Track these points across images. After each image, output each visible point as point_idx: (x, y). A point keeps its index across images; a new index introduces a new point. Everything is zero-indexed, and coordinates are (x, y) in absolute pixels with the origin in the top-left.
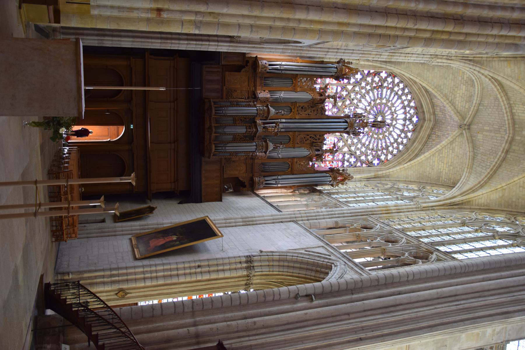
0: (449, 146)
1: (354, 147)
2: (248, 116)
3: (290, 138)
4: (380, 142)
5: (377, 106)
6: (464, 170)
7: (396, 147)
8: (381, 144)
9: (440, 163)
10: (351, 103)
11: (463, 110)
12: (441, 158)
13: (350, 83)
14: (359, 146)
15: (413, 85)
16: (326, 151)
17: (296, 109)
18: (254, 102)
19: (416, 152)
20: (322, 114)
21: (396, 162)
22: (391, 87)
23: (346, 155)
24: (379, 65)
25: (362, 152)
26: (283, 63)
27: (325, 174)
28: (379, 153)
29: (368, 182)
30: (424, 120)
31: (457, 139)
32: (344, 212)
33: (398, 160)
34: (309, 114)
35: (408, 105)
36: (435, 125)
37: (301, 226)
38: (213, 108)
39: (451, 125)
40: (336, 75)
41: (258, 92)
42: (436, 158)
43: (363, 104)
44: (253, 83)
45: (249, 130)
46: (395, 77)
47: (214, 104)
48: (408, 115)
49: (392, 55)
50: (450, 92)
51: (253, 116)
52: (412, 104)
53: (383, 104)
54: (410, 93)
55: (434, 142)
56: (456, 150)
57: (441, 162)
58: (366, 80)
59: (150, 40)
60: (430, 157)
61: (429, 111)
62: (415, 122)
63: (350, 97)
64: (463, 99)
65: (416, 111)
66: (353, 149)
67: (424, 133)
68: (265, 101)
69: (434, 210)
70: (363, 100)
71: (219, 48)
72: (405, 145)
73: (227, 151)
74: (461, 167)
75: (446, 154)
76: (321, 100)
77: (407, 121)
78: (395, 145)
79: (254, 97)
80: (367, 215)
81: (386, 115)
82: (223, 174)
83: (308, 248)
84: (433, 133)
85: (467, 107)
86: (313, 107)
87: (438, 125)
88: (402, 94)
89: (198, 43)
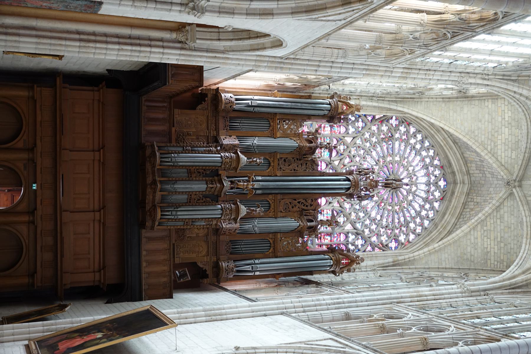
0: (495, 214)
1: (361, 224)
2: (209, 166)
3: (269, 204)
4: (396, 216)
5: (388, 164)
6: (521, 243)
7: (419, 223)
9: (485, 239)
10: (351, 161)
11: (509, 162)
12: (486, 232)
13: (348, 133)
15: (436, 134)
16: (322, 222)
17: (276, 162)
18: (216, 147)
19: (448, 228)
20: (314, 169)
21: (422, 243)
22: (405, 139)
23: (350, 235)
24: (388, 106)
25: (371, 231)
26: (256, 97)
27: (322, 256)
28: (397, 231)
29: (385, 271)
30: (455, 183)
31: (505, 204)
32: (357, 299)
33: (425, 240)
34: (294, 170)
36: (470, 189)
37: (294, 318)
38: (158, 154)
39: (494, 186)
40: (330, 114)
41: (222, 137)
42: (479, 233)
43: (368, 162)
44: (213, 125)
45: (211, 186)
46: (409, 124)
47: (159, 149)
49: (407, 73)
50: (488, 139)
51: (216, 166)
52: (436, 162)
53: (396, 162)
55: (474, 212)
56: (506, 219)
57: (486, 238)
59: (63, 42)
60: (470, 231)
61: (461, 170)
62: (442, 187)
63: (350, 152)
64: (507, 147)
65: (443, 171)
67: (457, 201)
68: (232, 148)
71: (164, 57)
72: (432, 220)
73: (180, 217)
74: (515, 242)
75: (493, 225)
76: (310, 148)
77: (432, 185)
78: (418, 220)
79: (216, 141)
80: (391, 303)
82: (174, 257)
83: (309, 341)
84: (469, 200)
85: (513, 157)
86: (300, 160)
87: (476, 188)
88: (421, 148)
89: (134, 48)
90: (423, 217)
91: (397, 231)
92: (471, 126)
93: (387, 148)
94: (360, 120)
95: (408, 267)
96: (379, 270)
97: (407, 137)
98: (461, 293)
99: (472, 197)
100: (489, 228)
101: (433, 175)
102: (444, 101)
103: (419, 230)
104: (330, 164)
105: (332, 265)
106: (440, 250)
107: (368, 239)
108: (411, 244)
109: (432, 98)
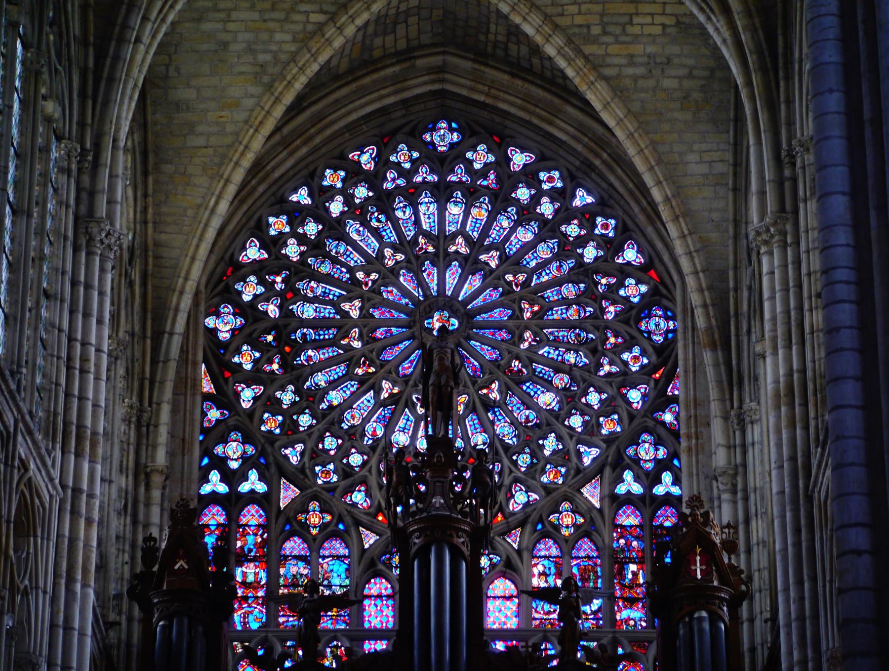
4: (556, 314)
5: (379, 344)
8: (566, 303)
9: (636, 30)
10: (364, 482)
12: (609, 29)
13: (265, 495)
14: (576, 421)
15: (267, 175)
23: (621, 489)
24: (172, 366)
25: (608, 408)
28: (611, 311)
35: (374, 180)
42: (613, 49)
43: (366, 420)
48: (423, 175)
50: (286, 20)
53: (365, 314)
54: (312, 181)
57: (630, 29)
58: (250, 413)
60: (606, 79)
65: (399, 136)
66: (595, 452)
69: (792, 157)
70: (352, 419)
75: (584, 8)
78: (573, 230)
81: (418, 293)
84: (500, 53)
88: (317, 221)
91: (611, 311)
92: (241, 73)
94: (219, 450)
95: (731, 294)
96: (741, 402)
97: (278, 274)
98: (784, 246)
99: (490, 45)
100: (596, 19)
101: (414, 171)
102: (157, 169)
103: (605, 226)
104: (372, 564)
105: (711, 613)
106: (670, 178)
107: (636, 422)
108: (656, 261)
109: (145, 210)
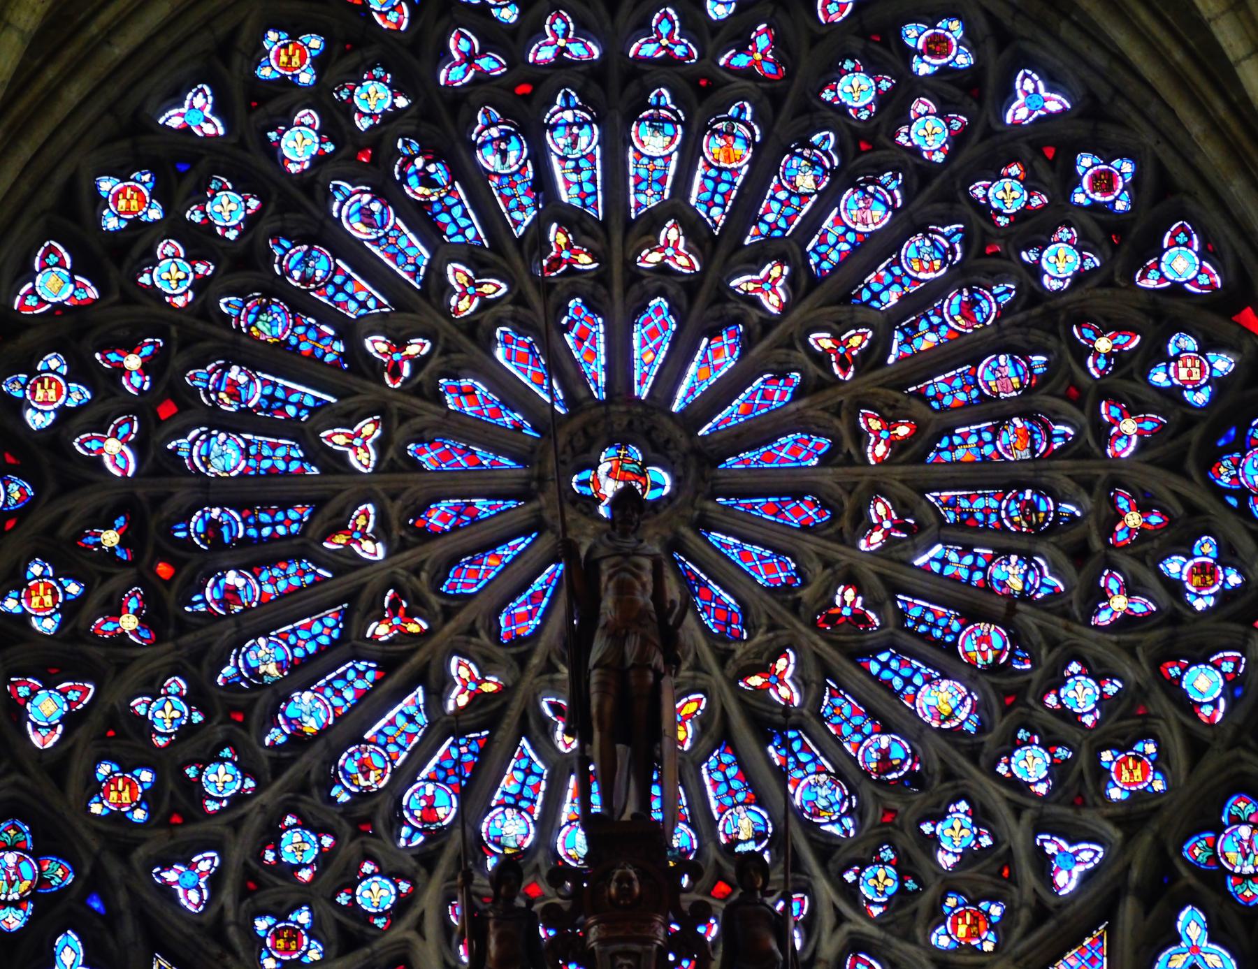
5: (436, 550)
43: (404, 776)
58: (56, 761)
66: (1089, 854)
90: (971, 151)
93: (252, 567)
97: (131, 347)
101: (530, 30)
103: (1104, 182)
107: (1210, 763)
